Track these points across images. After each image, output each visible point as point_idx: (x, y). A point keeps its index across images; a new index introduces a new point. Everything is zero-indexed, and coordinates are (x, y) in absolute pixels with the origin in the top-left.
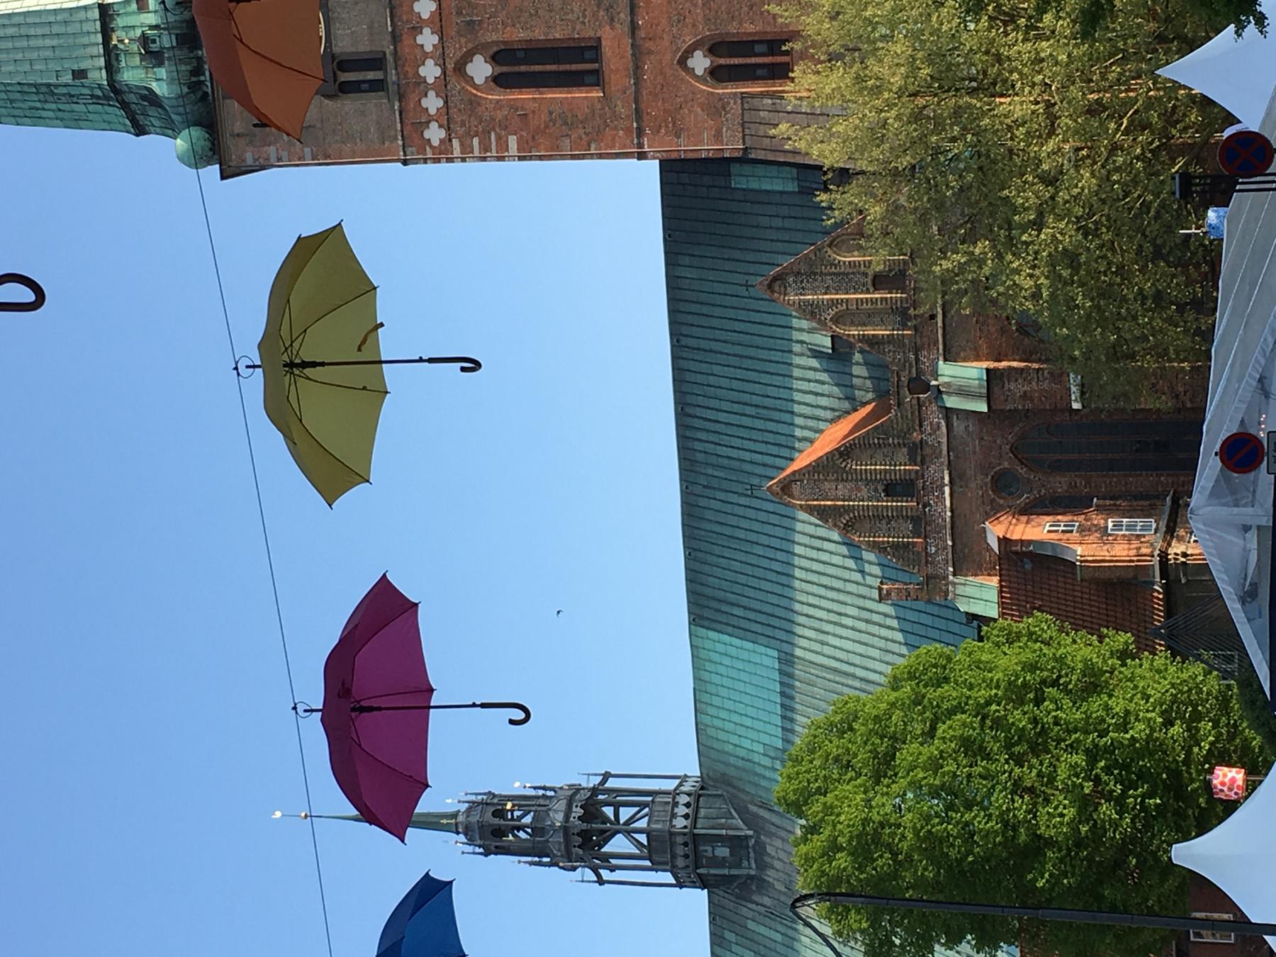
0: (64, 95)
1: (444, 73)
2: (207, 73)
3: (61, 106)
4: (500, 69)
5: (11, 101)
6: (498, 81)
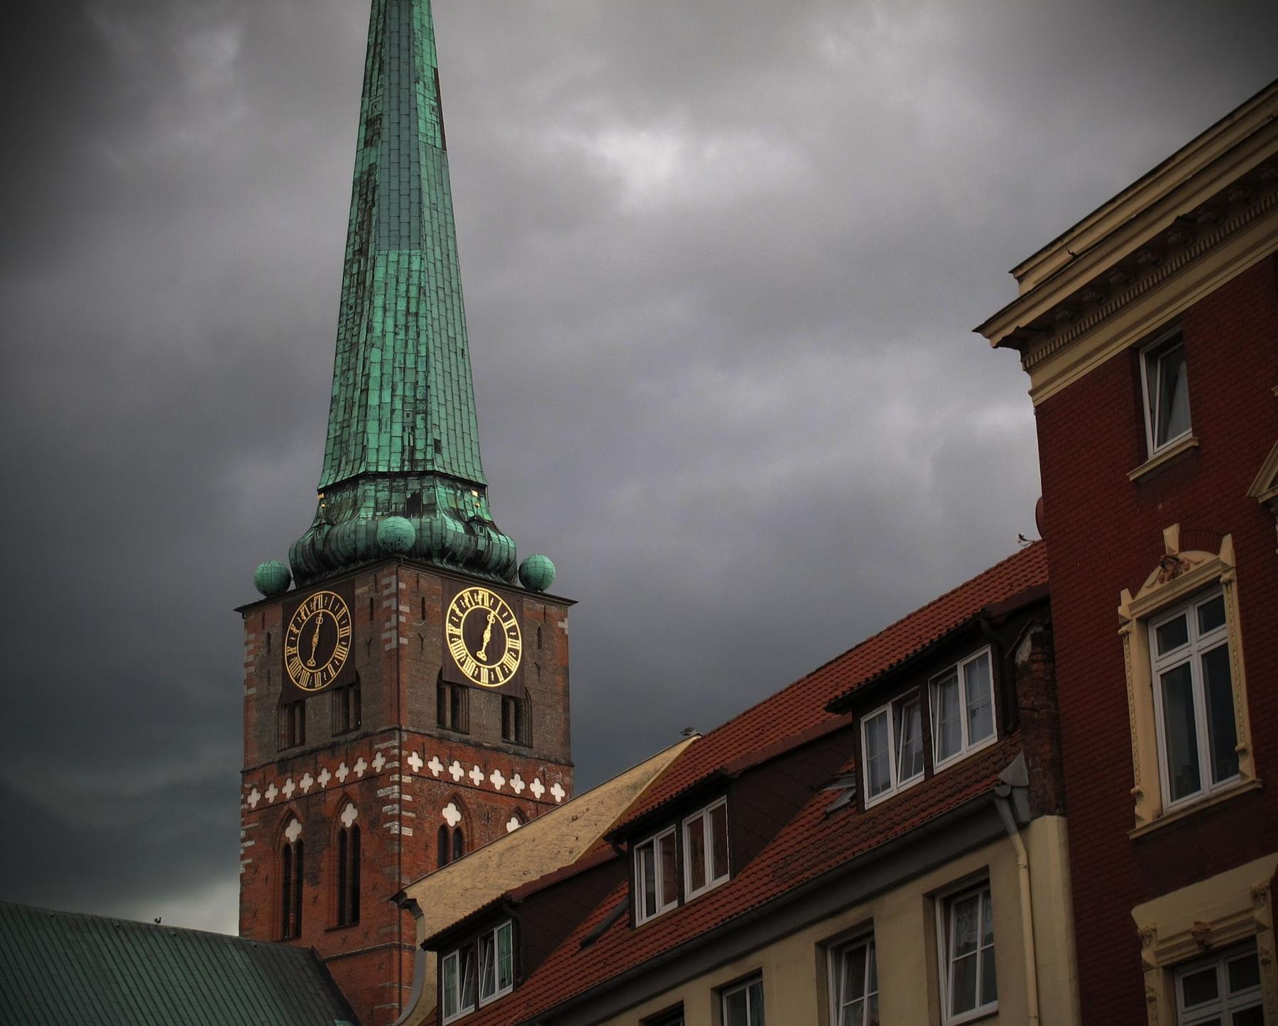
0: (414, 422)
1: (455, 784)
2: (450, 567)
3: (398, 414)
4: (452, 833)
5: (404, 370)
6: (444, 827)
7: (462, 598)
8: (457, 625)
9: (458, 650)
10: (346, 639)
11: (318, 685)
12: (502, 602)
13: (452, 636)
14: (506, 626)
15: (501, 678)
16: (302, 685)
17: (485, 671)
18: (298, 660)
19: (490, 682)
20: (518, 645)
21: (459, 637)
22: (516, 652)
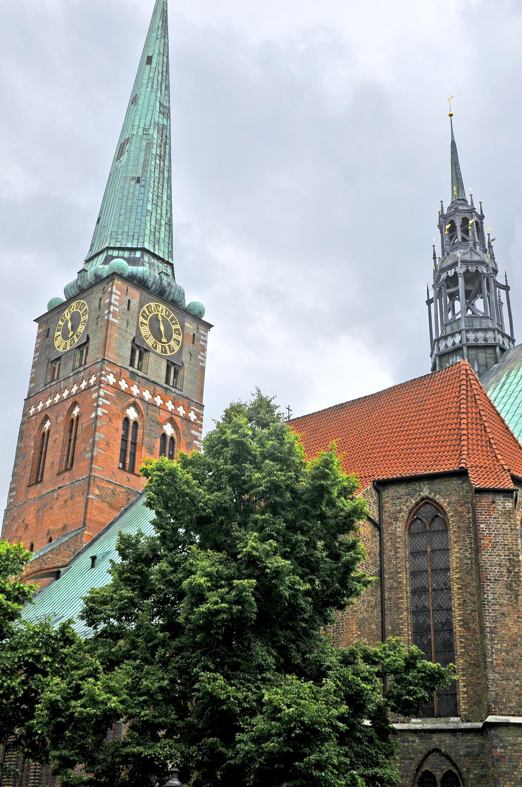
8: (146, 319)
10: (85, 321)
11: (68, 348)
12: (172, 315)
13: (142, 323)
14: (174, 327)
15: (169, 352)
16: (61, 350)
18: (60, 338)
19: (162, 352)
20: (180, 338)
21: (146, 325)
22: (178, 342)
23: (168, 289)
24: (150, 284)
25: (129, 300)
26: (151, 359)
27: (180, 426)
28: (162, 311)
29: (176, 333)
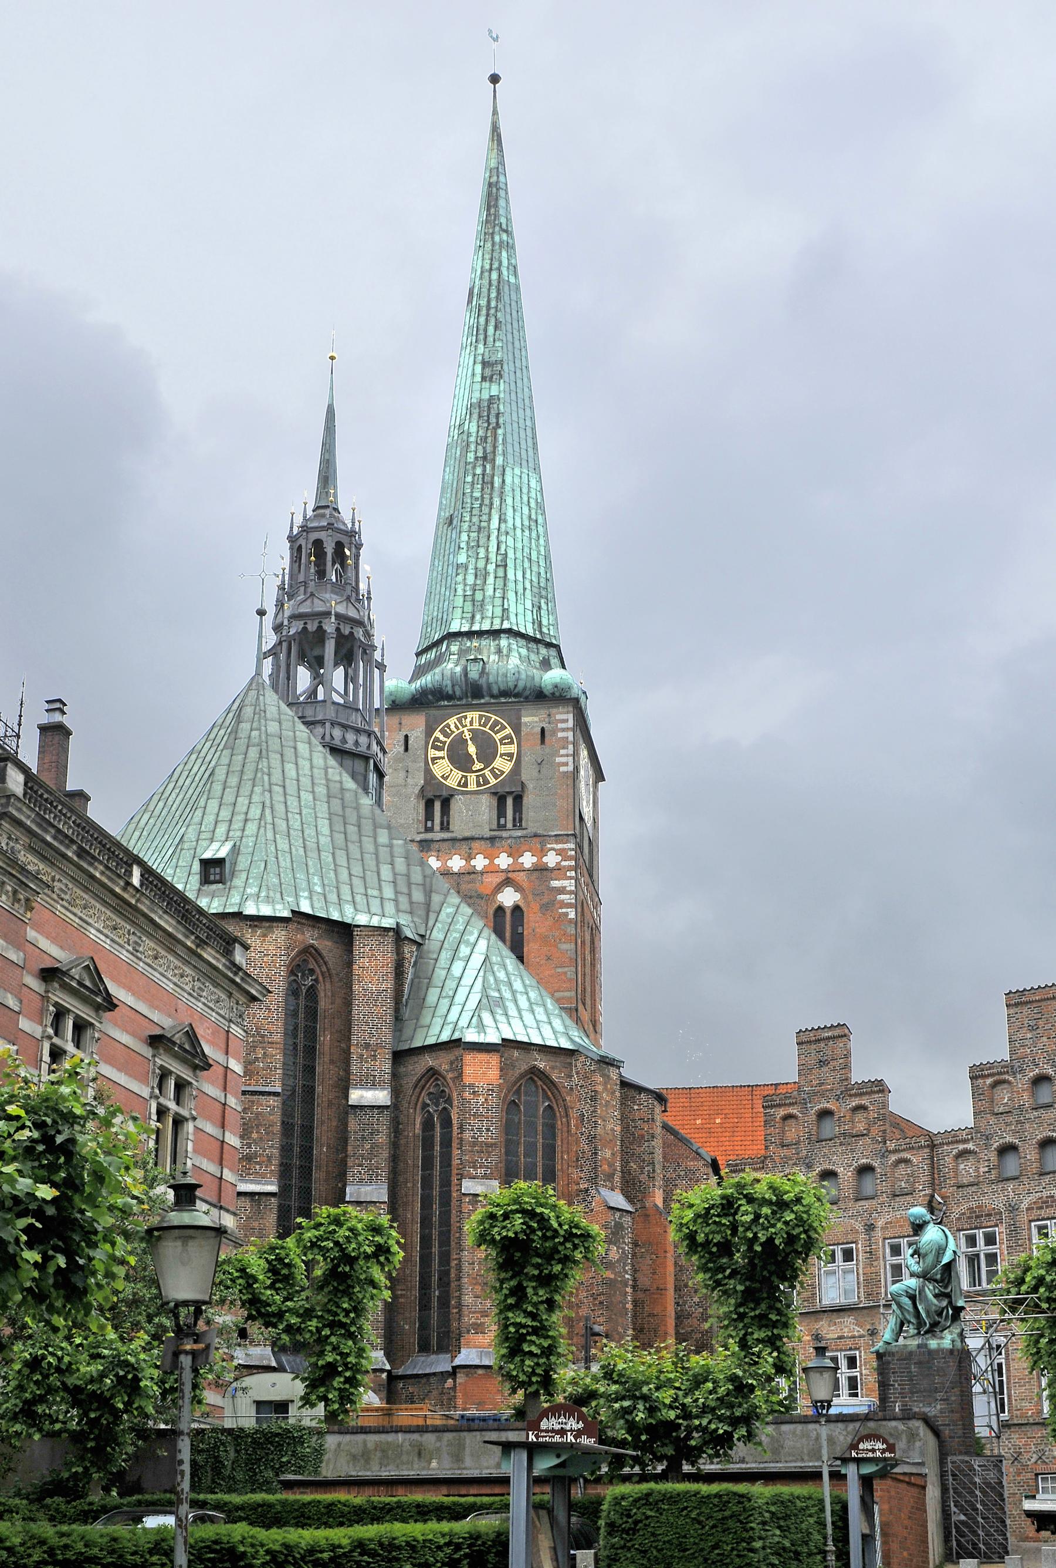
7: (448, 726)
9: (442, 768)
12: (494, 717)
13: (434, 759)
14: (497, 737)
17: (472, 778)
21: (443, 758)
23: (483, 681)
24: (449, 689)
25: (406, 737)
26: (458, 805)
27: (525, 885)
28: (471, 723)
29: (505, 744)
